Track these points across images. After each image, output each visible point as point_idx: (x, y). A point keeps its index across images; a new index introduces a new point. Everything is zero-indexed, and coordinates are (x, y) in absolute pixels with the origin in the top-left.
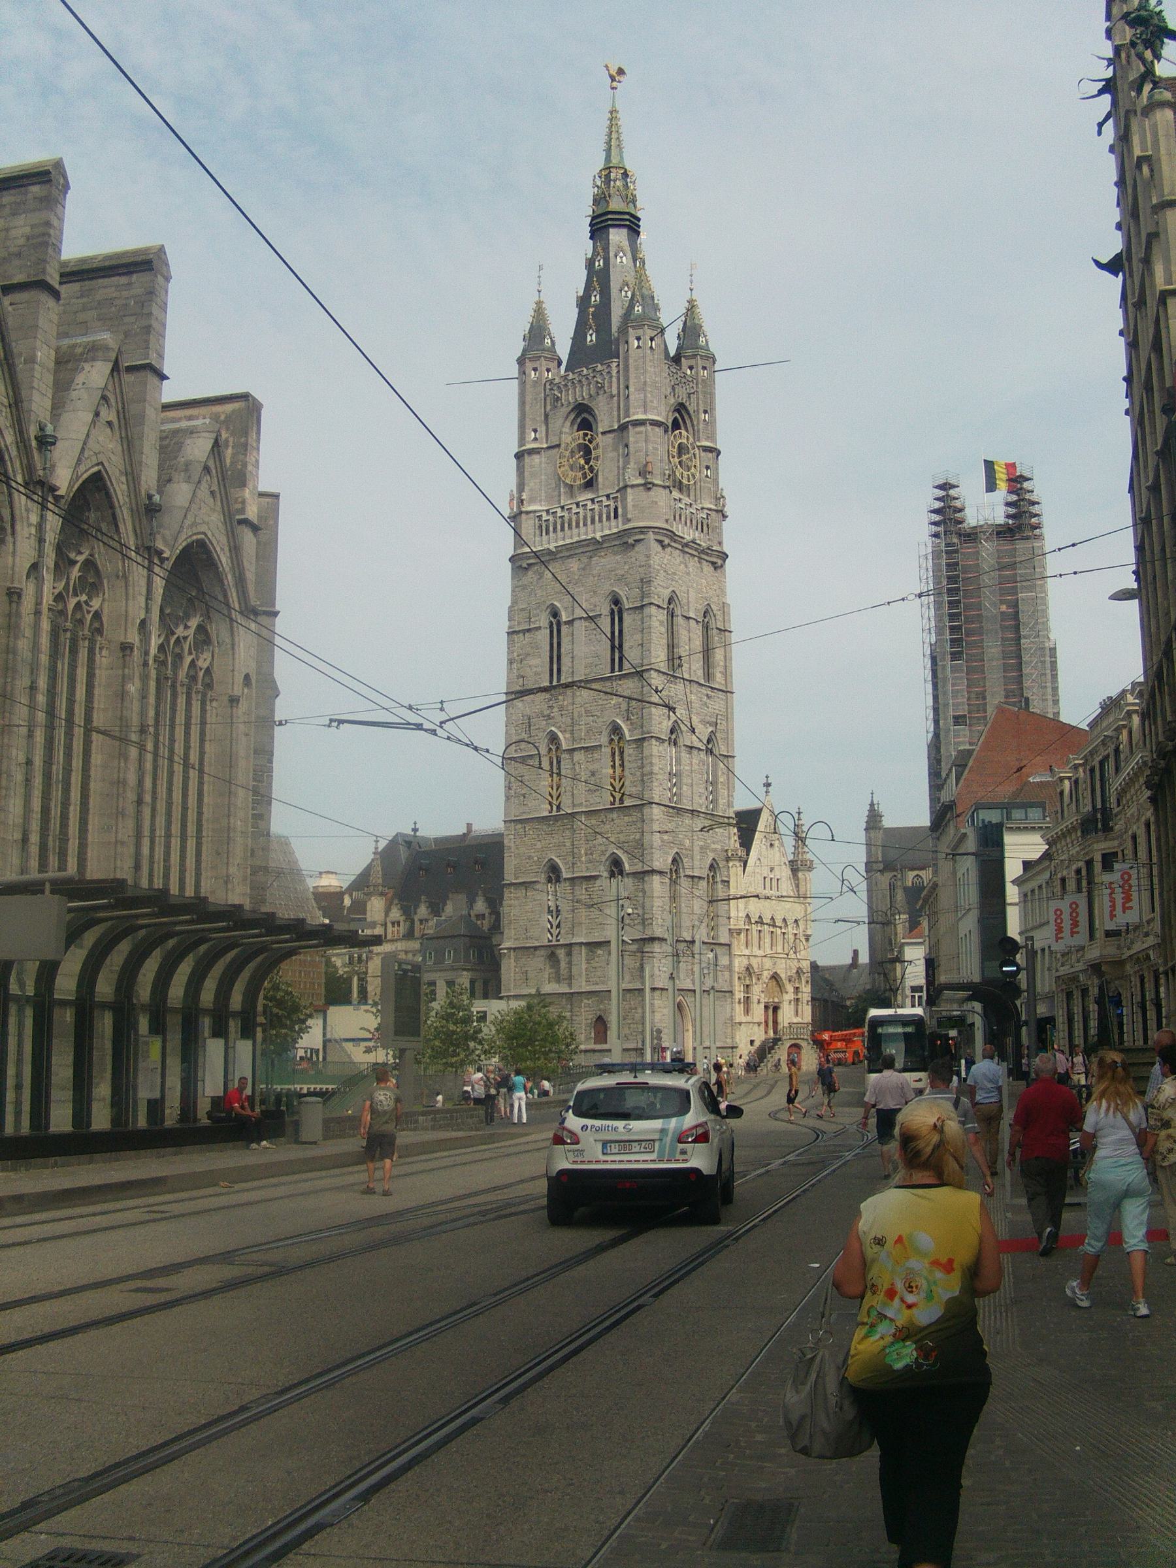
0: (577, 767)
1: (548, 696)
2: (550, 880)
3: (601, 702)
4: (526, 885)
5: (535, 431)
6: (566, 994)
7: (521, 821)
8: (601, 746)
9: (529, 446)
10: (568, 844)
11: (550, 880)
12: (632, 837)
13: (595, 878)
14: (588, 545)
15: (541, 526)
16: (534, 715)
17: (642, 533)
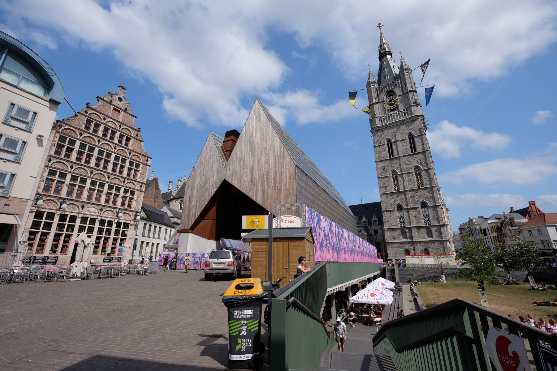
0: (404, 178)
1: (390, 161)
2: (398, 209)
3: (410, 161)
4: (390, 211)
5: (375, 99)
6: (411, 242)
7: (386, 194)
8: (412, 172)
9: (374, 102)
10: (404, 199)
11: (398, 209)
12: (429, 196)
13: (416, 208)
14: (399, 122)
15: (381, 120)
16: (386, 166)
17: (418, 117)
